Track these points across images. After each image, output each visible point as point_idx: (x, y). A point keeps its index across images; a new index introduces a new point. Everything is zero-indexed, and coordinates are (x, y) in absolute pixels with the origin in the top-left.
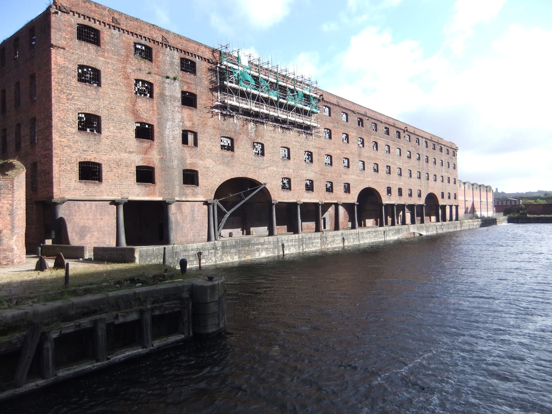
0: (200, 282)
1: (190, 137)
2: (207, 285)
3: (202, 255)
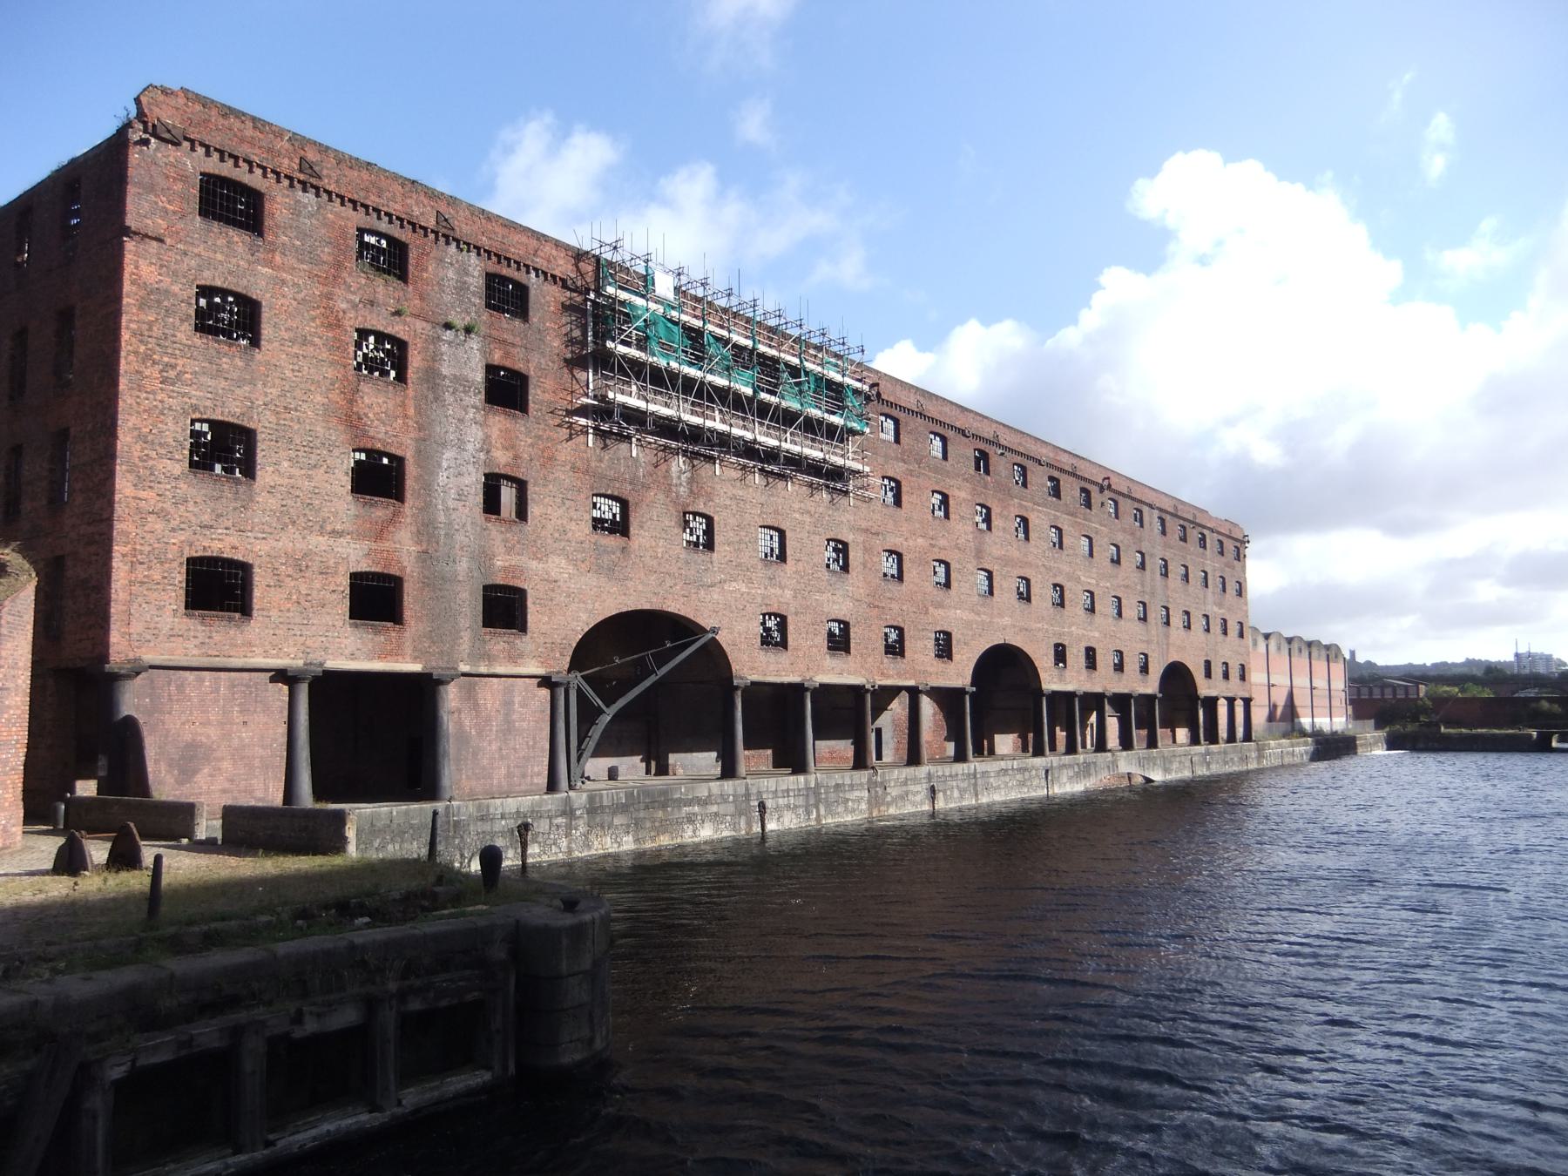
0: (540, 914)
1: (507, 495)
2: (560, 923)
3: (530, 833)
